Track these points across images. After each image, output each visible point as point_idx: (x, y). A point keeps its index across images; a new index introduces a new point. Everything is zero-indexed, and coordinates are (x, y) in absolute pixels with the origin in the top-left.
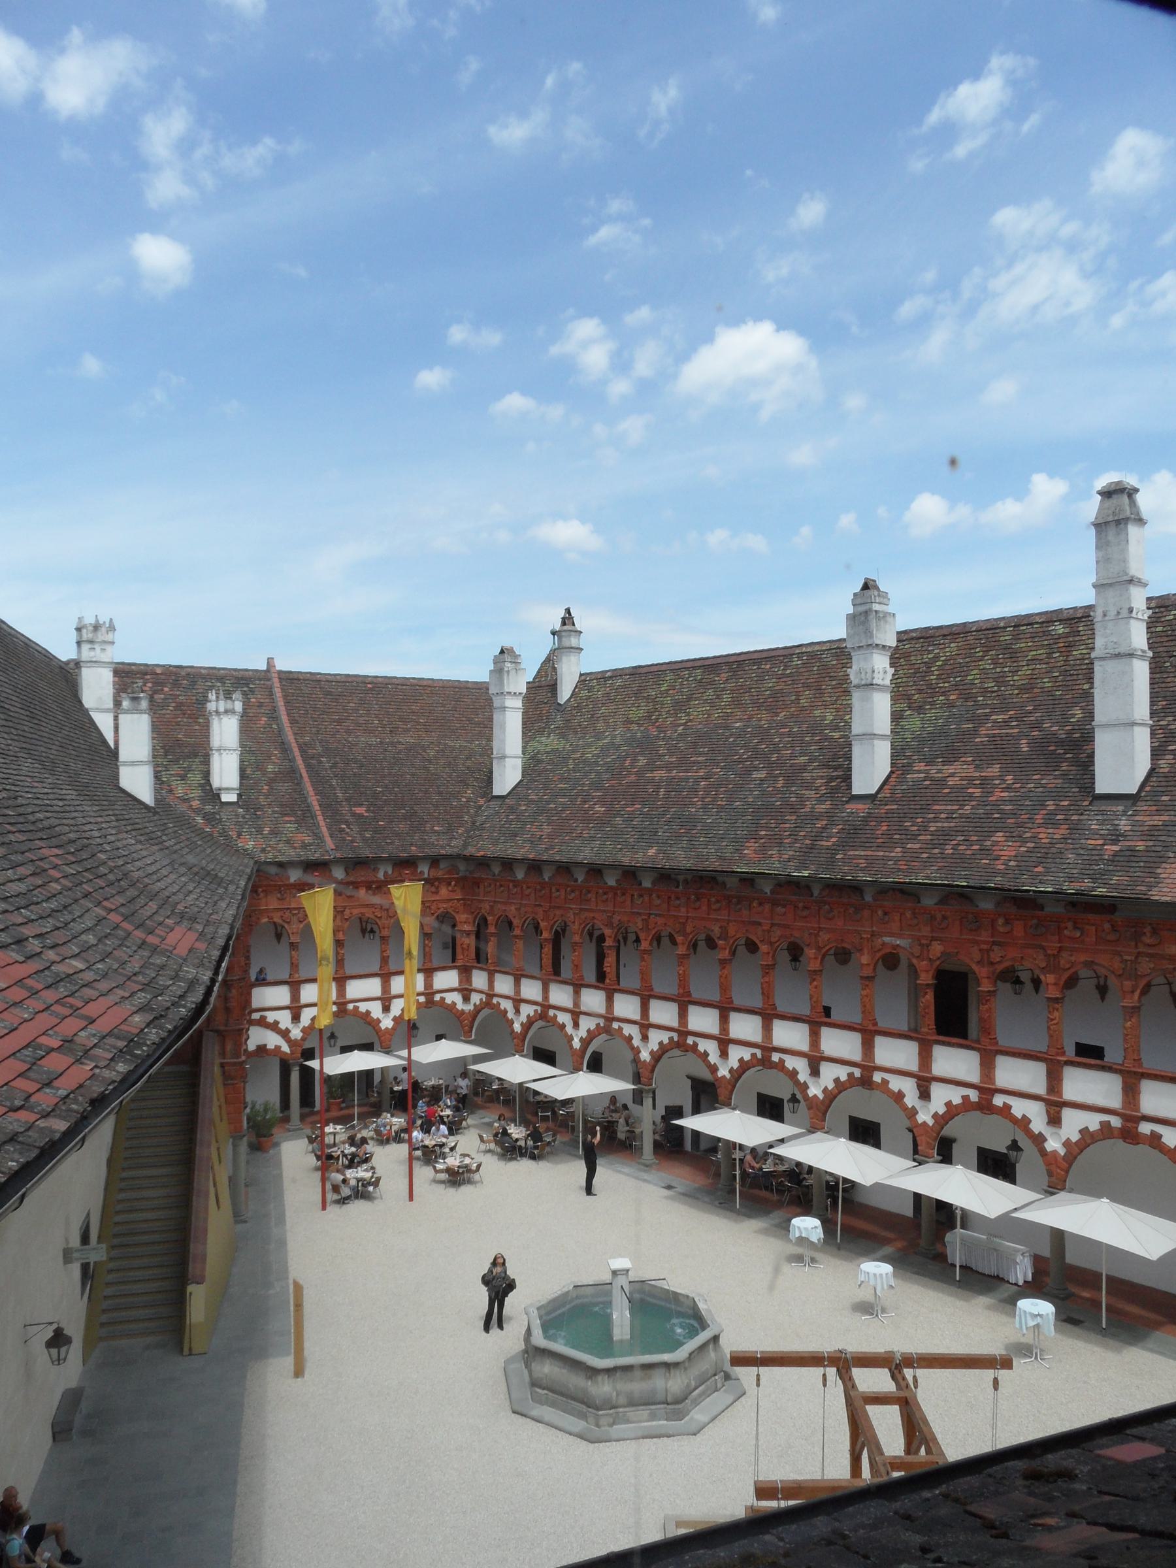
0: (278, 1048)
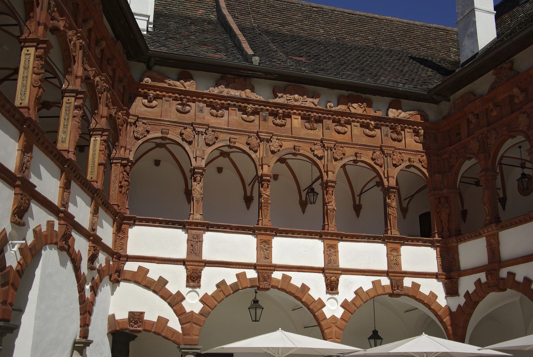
0: (162, 321)
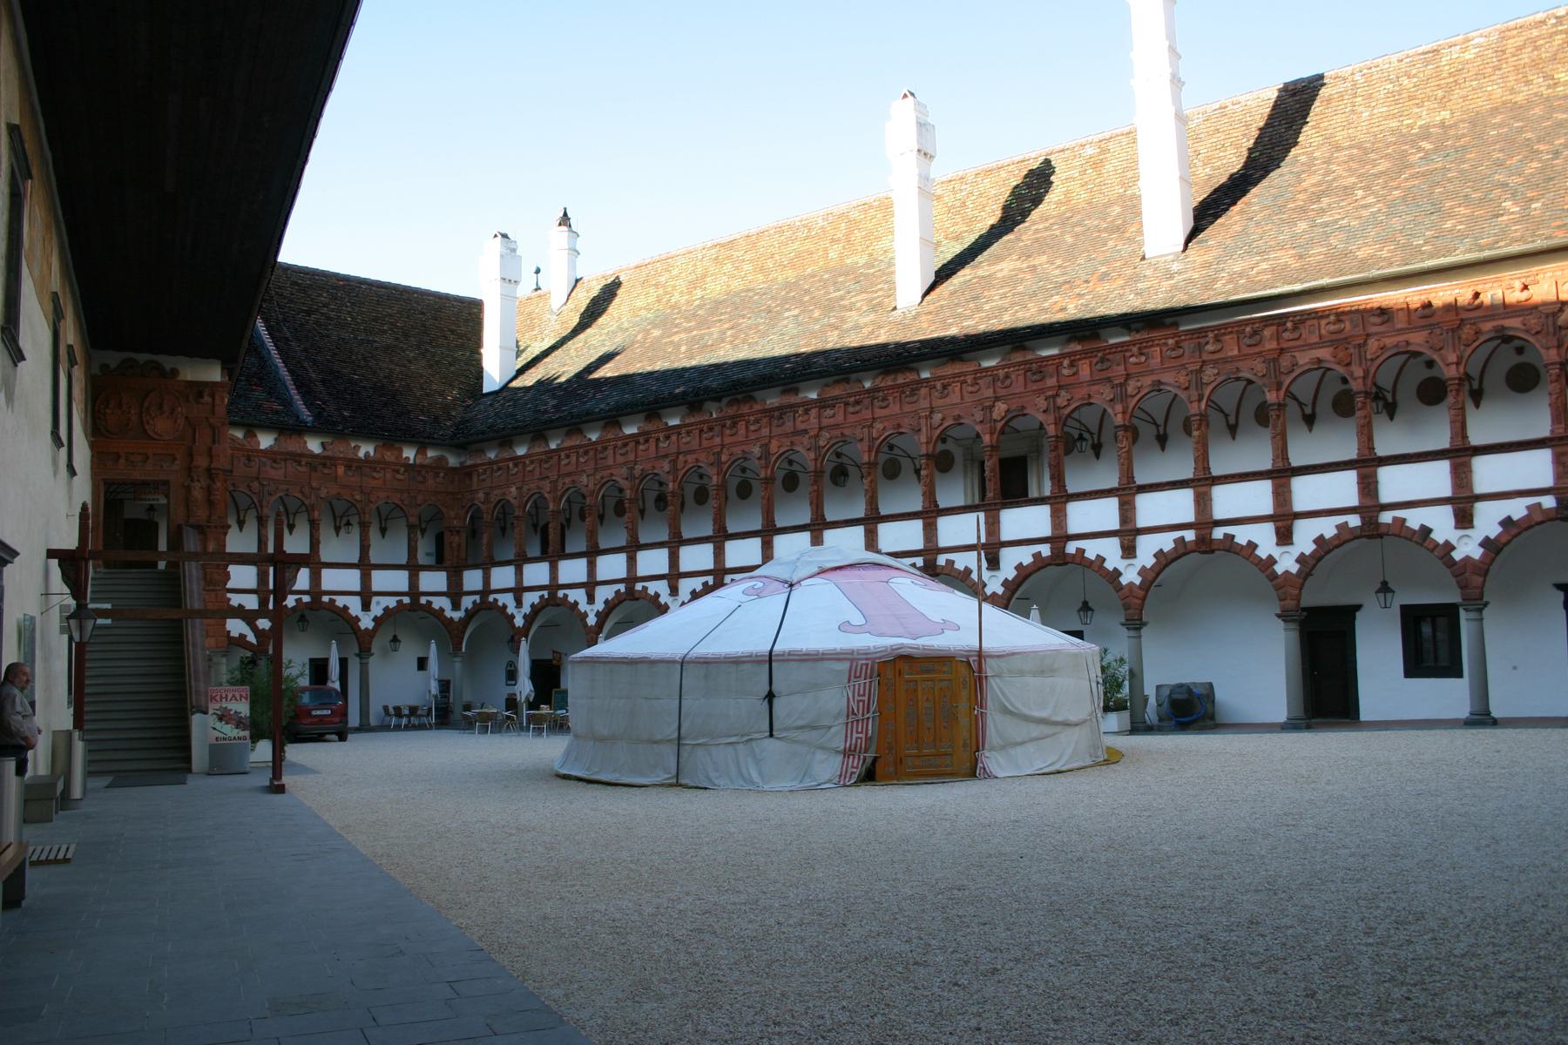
0: (242, 636)
